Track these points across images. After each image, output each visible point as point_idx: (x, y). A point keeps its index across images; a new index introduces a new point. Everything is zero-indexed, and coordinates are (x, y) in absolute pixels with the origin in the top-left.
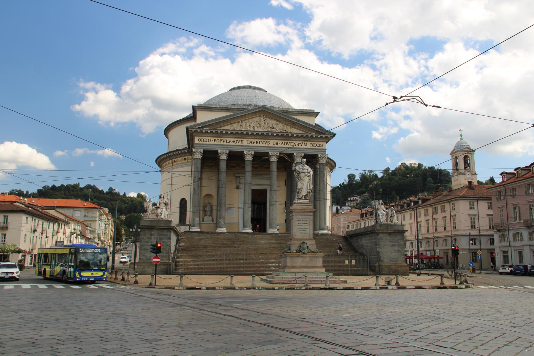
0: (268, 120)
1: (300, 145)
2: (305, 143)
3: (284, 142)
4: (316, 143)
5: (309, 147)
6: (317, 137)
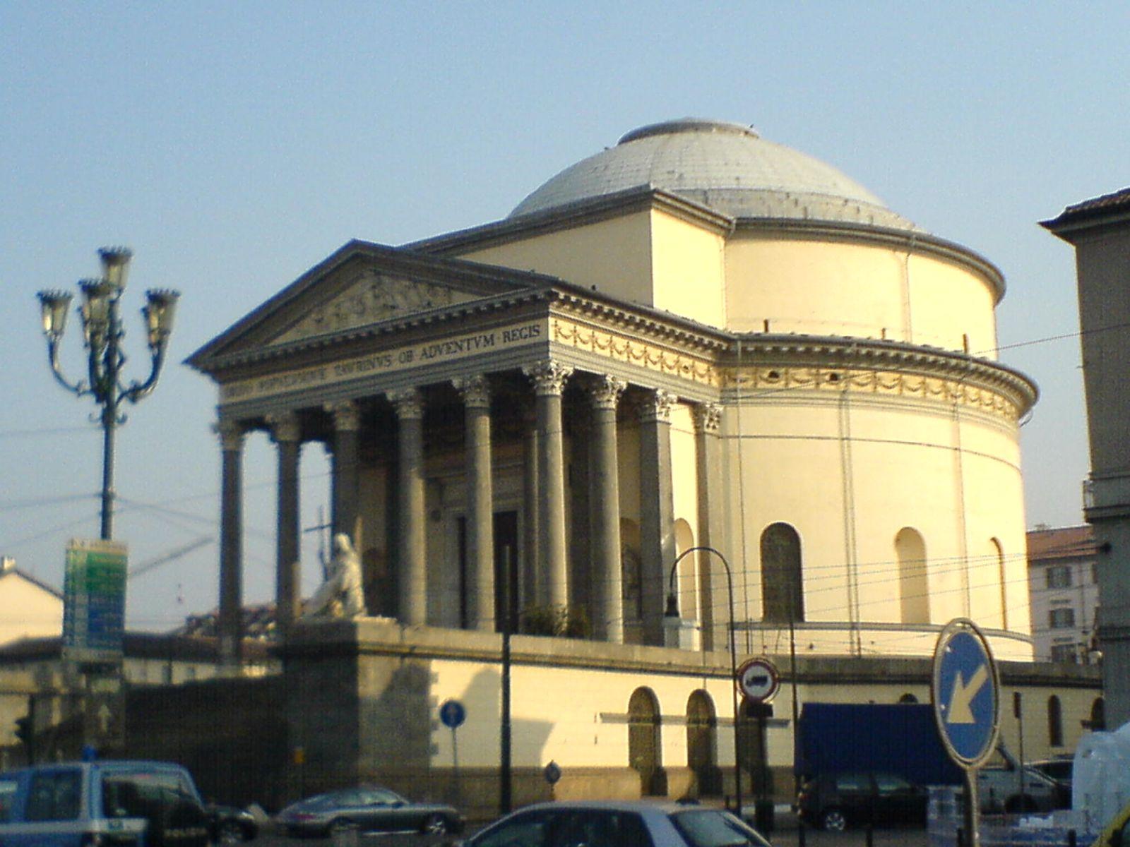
0: (386, 280)
1: (473, 343)
2: (488, 334)
3: (427, 346)
4: (520, 326)
5: (496, 343)
6: (506, 305)
